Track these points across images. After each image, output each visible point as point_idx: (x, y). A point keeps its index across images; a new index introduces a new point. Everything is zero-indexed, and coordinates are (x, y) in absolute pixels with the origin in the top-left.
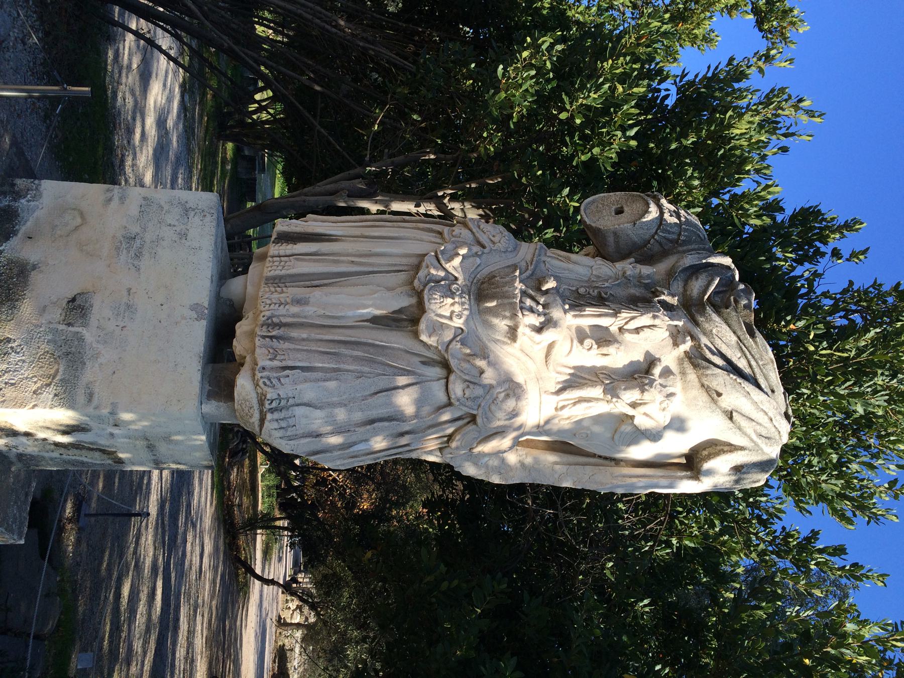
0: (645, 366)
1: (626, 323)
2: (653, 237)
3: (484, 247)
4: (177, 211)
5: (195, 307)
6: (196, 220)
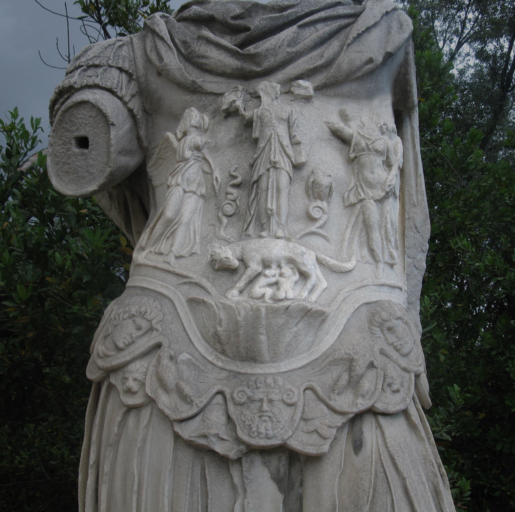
0: (336, 143)
1: (288, 156)
2: (125, 104)
3: (158, 346)
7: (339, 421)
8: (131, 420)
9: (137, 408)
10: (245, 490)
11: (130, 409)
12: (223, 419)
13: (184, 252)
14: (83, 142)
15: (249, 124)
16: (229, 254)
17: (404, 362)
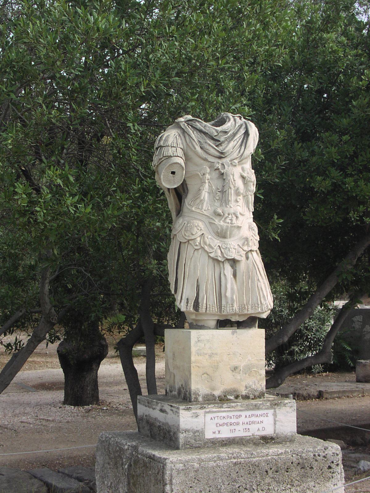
0: (242, 178)
3: (203, 234)
4: (199, 344)
5: (233, 333)
6: (202, 338)
7: (245, 253)
8: (196, 252)
9: (198, 249)
10: (224, 269)
11: (196, 249)
12: (220, 252)
13: (206, 209)
14: (173, 173)
15: (223, 174)
16: (220, 211)
17: (256, 238)
